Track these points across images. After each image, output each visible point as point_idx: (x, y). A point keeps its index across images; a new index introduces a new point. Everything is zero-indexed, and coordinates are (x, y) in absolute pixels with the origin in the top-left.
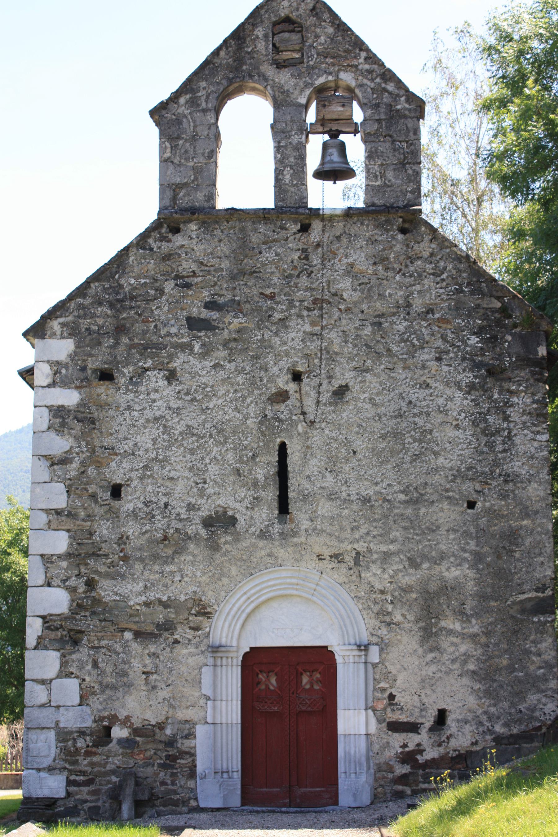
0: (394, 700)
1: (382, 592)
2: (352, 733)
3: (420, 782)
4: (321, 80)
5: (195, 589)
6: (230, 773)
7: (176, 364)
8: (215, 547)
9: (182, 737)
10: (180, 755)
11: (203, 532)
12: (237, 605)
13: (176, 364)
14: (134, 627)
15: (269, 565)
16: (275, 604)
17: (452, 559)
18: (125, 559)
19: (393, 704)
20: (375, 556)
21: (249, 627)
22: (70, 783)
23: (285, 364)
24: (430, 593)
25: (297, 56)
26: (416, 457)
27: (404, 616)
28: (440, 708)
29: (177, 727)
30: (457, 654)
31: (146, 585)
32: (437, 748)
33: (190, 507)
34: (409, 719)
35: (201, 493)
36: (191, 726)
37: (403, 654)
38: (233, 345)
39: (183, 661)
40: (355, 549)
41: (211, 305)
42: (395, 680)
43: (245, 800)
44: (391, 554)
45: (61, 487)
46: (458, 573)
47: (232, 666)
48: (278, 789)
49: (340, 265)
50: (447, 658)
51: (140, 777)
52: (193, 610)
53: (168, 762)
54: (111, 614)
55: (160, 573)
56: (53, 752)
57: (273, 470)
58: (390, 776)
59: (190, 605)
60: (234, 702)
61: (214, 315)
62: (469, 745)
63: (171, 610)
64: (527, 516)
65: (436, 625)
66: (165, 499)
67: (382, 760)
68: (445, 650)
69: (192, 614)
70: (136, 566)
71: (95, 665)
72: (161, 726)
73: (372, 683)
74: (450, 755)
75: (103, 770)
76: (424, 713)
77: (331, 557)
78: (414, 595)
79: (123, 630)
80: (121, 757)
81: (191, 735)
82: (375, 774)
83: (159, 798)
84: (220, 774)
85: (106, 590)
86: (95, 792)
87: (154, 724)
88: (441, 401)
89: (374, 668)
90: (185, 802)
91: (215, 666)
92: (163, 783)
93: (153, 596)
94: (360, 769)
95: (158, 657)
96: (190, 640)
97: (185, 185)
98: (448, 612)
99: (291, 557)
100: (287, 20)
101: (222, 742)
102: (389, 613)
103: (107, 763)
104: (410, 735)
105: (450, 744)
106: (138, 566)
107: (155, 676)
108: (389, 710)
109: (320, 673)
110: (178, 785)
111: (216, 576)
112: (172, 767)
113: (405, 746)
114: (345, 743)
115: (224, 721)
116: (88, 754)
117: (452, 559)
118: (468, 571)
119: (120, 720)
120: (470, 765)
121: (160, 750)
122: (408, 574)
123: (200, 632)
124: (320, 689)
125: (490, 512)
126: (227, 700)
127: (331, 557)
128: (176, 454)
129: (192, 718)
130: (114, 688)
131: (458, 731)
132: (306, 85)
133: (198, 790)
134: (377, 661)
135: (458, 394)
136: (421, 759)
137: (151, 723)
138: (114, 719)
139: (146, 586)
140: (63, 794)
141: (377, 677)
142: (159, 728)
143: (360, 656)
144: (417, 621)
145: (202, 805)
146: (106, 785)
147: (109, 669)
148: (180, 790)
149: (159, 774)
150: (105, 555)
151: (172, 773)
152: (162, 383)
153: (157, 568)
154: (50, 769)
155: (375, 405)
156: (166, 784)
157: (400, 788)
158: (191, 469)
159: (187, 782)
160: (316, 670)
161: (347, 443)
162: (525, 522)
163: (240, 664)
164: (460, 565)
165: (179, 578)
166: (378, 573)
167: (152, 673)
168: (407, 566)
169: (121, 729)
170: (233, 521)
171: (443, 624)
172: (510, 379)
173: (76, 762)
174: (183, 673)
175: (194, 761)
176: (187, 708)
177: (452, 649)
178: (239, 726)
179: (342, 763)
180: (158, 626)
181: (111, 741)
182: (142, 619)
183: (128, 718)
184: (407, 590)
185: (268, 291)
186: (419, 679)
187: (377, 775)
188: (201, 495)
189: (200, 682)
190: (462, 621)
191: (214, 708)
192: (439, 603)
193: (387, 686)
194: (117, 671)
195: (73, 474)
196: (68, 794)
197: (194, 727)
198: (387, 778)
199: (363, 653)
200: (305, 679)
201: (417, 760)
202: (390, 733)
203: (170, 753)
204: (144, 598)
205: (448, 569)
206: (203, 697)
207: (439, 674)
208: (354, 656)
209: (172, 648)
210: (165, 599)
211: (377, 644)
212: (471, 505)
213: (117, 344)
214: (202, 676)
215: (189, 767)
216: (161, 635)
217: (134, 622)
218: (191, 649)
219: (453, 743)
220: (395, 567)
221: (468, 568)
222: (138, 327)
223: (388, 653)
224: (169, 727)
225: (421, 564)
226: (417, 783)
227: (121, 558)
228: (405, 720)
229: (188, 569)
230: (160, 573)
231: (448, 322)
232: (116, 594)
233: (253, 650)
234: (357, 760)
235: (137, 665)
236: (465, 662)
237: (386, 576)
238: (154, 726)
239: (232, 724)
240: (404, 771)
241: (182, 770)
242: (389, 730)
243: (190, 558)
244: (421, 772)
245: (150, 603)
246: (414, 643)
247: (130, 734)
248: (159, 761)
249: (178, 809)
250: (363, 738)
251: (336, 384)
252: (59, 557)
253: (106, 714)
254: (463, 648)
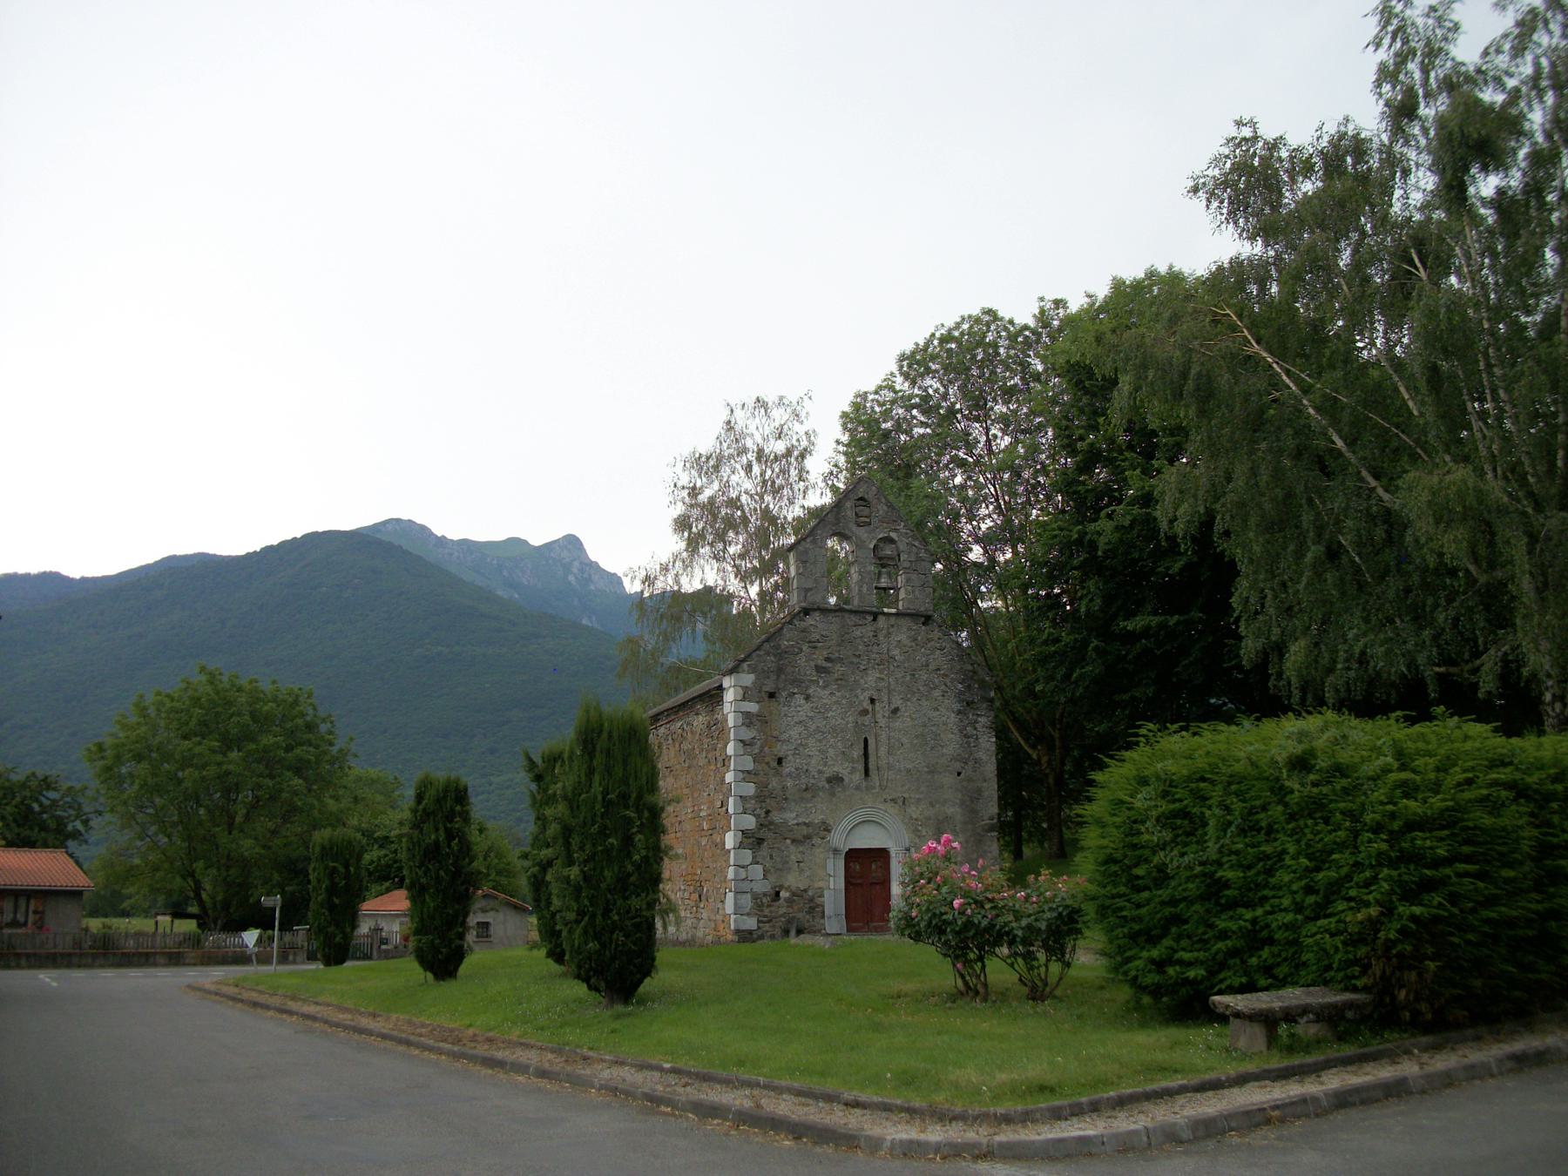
4: (881, 536)
7: (810, 691)
8: (833, 795)
11: (827, 786)
13: (810, 691)
18: (786, 799)
22: (759, 922)
23: (867, 694)
25: (868, 520)
26: (932, 748)
33: (820, 772)
35: (825, 764)
38: (839, 682)
41: (827, 659)
43: (848, 931)
45: (750, 758)
49: (895, 638)
56: (750, 905)
57: (862, 752)
61: (829, 665)
64: (985, 781)
66: (805, 767)
71: (771, 857)
72: (805, 891)
81: (822, 896)
86: (774, 926)
88: (944, 719)
93: (801, 820)
97: (811, 589)
100: (861, 499)
116: (769, 906)
125: (970, 780)
128: (811, 742)
130: (781, 870)
132: (873, 538)
135: (953, 715)
138: (781, 887)
140: (756, 928)
147: (778, 859)
152: (803, 702)
154: (748, 914)
155: (912, 719)
158: (819, 751)
161: (899, 740)
162: (985, 784)
170: (842, 779)
172: (977, 709)
173: (762, 911)
180: (804, 837)
183: (789, 886)
184: (928, 818)
185: (857, 653)
188: (825, 766)
195: (757, 751)
196: (759, 928)
200: (873, 867)
204: (795, 822)
212: (959, 774)
213: (778, 676)
222: (789, 669)
231: (946, 676)
233: (850, 850)
235: (793, 857)
251: (893, 707)
252: (750, 797)
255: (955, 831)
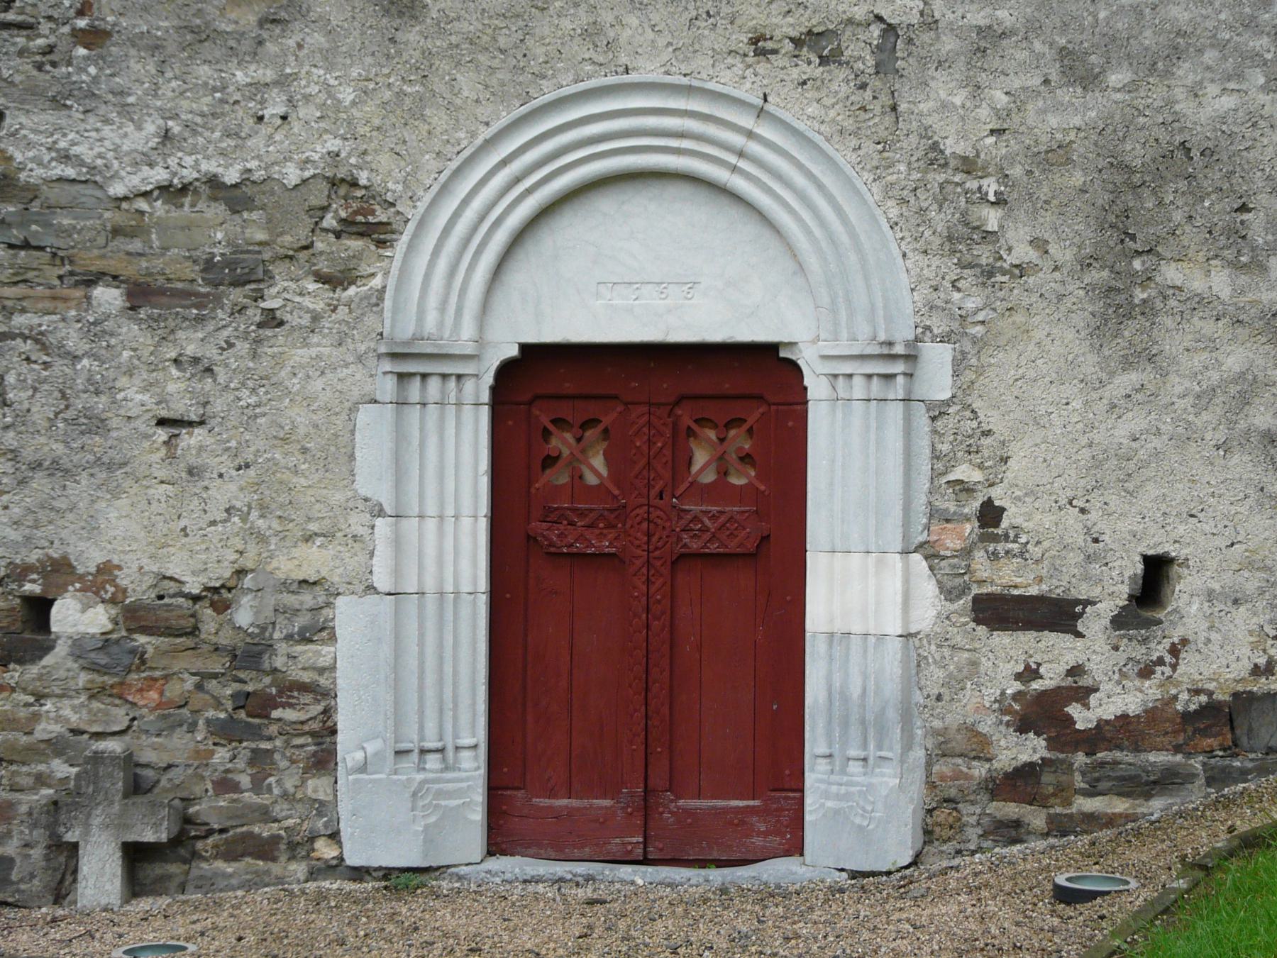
0: (997, 525)
1: (968, 166)
2: (857, 628)
3: (1077, 792)
5: (333, 144)
6: (450, 753)
9: (289, 637)
10: (281, 693)
12: (477, 204)
14: (129, 270)
15: (588, 68)
16: (605, 204)
17: (1210, 56)
19: (995, 539)
20: (949, 44)
21: (520, 277)
24: (1129, 170)
27: (1039, 244)
28: (1151, 552)
29: (271, 600)
30: (1215, 376)
31: (167, 131)
32: (1137, 683)
34: (1044, 587)
36: (321, 600)
37: (1031, 374)
39: (295, 384)
40: (879, 18)
42: (1005, 460)
44: (1003, 35)
46: (1228, 102)
47: (459, 404)
48: (607, 803)
50: (1179, 389)
51: (147, 766)
52: (329, 216)
53: (242, 715)
54: (47, 225)
55: (215, 89)
58: (979, 770)
59: (317, 200)
60: (466, 522)
62: (1244, 673)
63: (255, 215)
65: (1147, 279)
67: (953, 720)
68: (1174, 361)
69: (326, 230)
70: (135, 66)
73: (925, 468)
74: (1179, 707)
75: (24, 739)
76: (1095, 568)
77: (797, 42)
78: (1078, 179)
79: (91, 281)
80: (83, 698)
82: (929, 765)
83: (210, 832)
84: (415, 756)
85: (30, 145)
87: (196, 591)
89: (933, 419)
90: (299, 846)
91: (401, 403)
92: (225, 785)
93: (188, 167)
94: (880, 748)
95: (209, 370)
96: (316, 317)
98: (1190, 236)
99: (661, 42)
101: (421, 653)
102: (988, 236)
103: (36, 717)
104: (1051, 639)
105: (1181, 669)
106: (140, 67)
107: (199, 434)
108: (979, 555)
109: (750, 431)
110: (276, 791)
111: (408, 101)
112: (256, 733)
113: (1030, 673)
114: (831, 658)
115: (430, 585)
117: (1210, 56)
118: (1263, 98)
119: (81, 578)
120: (1244, 740)
121: (215, 676)
122: (1059, 107)
123: (352, 290)
124: (749, 485)
126: (441, 517)
127: (797, 42)
129: (324, 573)
130: (57, 469)
131: (1211, 628)
133: (344, 808)
134: (946, 395)
136: (1083, 718)
137: (186, 590)
139: (166, 136)
141: (945, 448)
142: (213, 605)
143: (889, 377)
144: (1086, 264)
145: (352, 860)
146: (34, 789)
147: (41, 411)
148: (279, 810)
149: (212, 753)
150: (20, 26)
151: (253, 751)
153: (204, 71)
156: (235, 787)
157: (1010, 810)
159: (304, 781)
160: (736, 422)
163: (485, 396)
164: (1239, 76)
165: (281, 110)
166: (958, 101)
167: (190, 424)
168: (1054, 77)
169: (85, 608)
171: (1171, 273)
174: (294, 427)
175: (328, 712)
176: (308, 539)
177: (1199, 360)
178: (483, 601)
179: (821, 724)
180: (209, 265)
181: (48, 648)
182: (156, 244)
183: (106, 570)
186: (1086, 453)
187: (936, 769)
189: (352, 457)
190: (1236, 266)
191: (397, 542)
192: (1160, 203)
193: (976, 476)
194: (70, 414)
197: (328, 605)
198: (968, 777)
199: (899, 367)
201: (1070, 721)
202: (982, 630)
203: (250, 688)
204: (159, 175)
205: (1195, 92)
206: (361, 505)
207: (1156, 442)
208: (869, 376)
209: (258, 341)
210: (231, 176)
211: (945, 338)
214: (358, 436)
215: (313, 734)
216: (218, 300)
217: (129, 254)
218: (321, 346)
219: (1191, 668)
220: (1016, 83)
221: (1265, 89)
223: (980, 371)
224: (246, 600)
225: (1103, 72)
226: (1064, 793)
227: (81, 37)
228: (1033, 591)
229: (313, 78)
230: (215, 89)
232: (65, 157)
234: (870, 717)
236: (1244, 400)
237: (984, 112)
238: (196, 599)
239: (457, 593)
240: (1024, 758)
241: (287, 742)
242: (978, 621)
243: (317, 39)
244: (1080, 759)
245: (184, 189)
246: (1070, 335)
247: (115, 622)
248: (211, 713)
249: (276, 869)
250: (894, 648)
253: (34, 557)
254: (1234, 360)
255: (1238, 235)
